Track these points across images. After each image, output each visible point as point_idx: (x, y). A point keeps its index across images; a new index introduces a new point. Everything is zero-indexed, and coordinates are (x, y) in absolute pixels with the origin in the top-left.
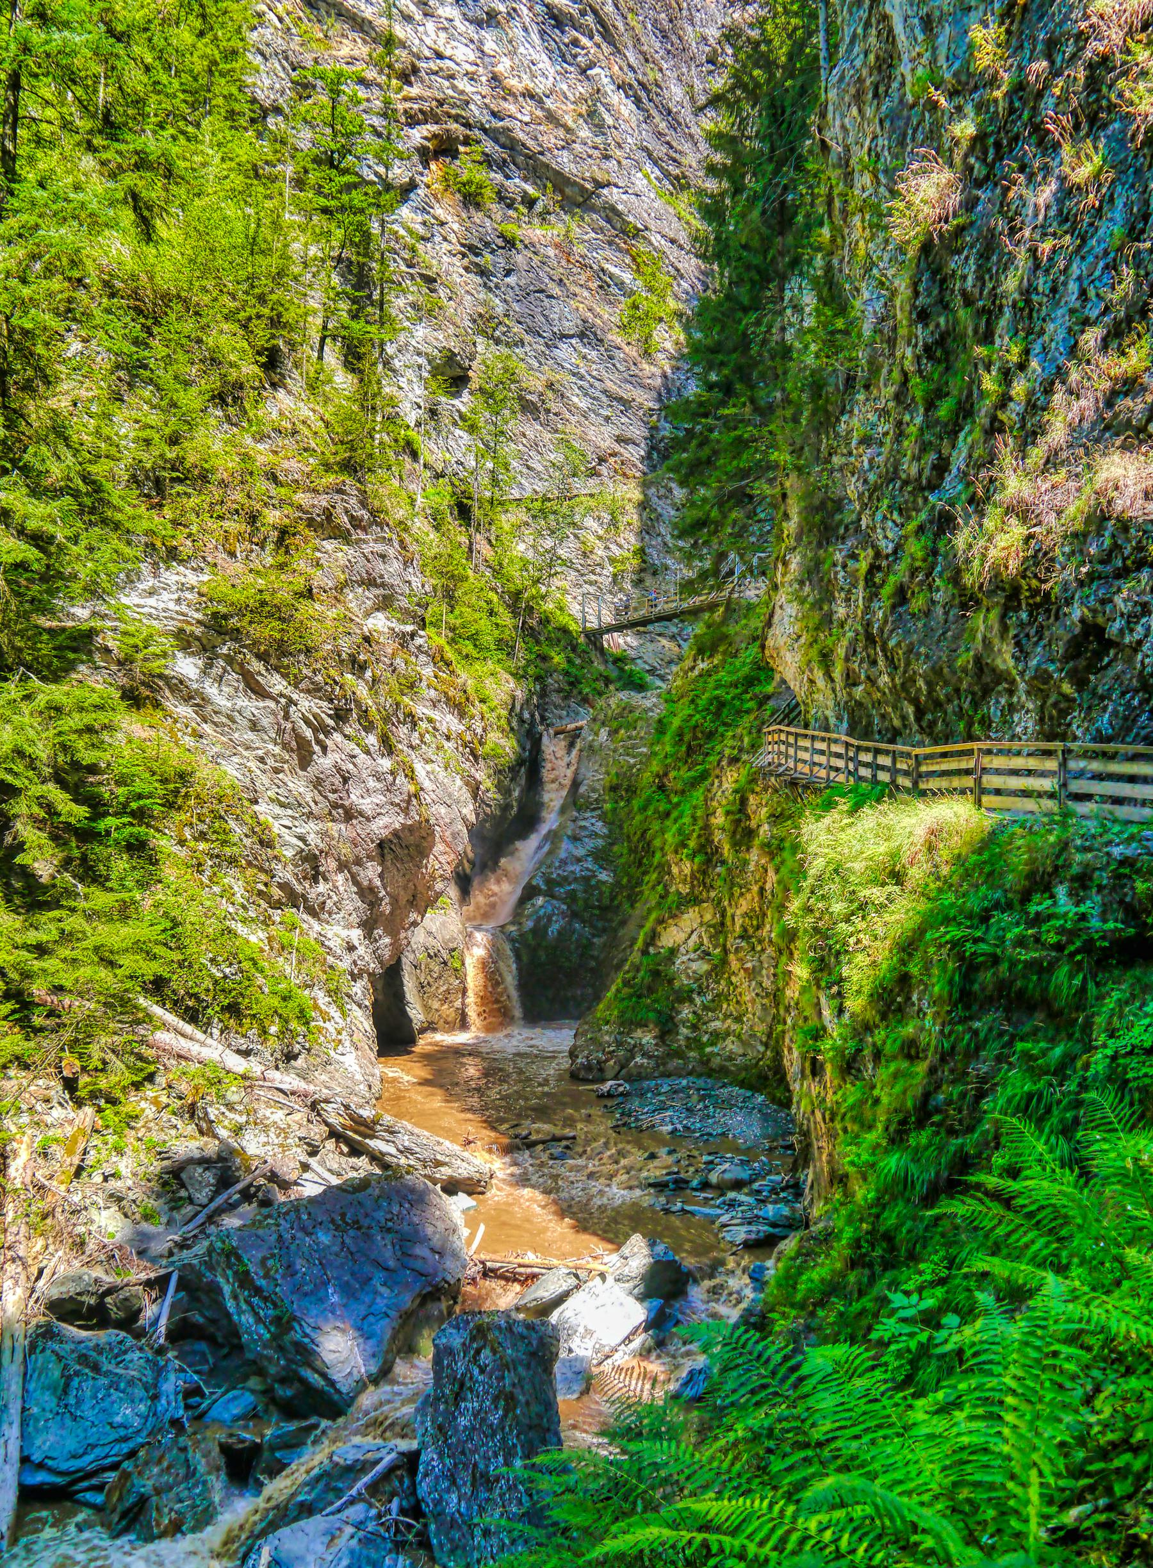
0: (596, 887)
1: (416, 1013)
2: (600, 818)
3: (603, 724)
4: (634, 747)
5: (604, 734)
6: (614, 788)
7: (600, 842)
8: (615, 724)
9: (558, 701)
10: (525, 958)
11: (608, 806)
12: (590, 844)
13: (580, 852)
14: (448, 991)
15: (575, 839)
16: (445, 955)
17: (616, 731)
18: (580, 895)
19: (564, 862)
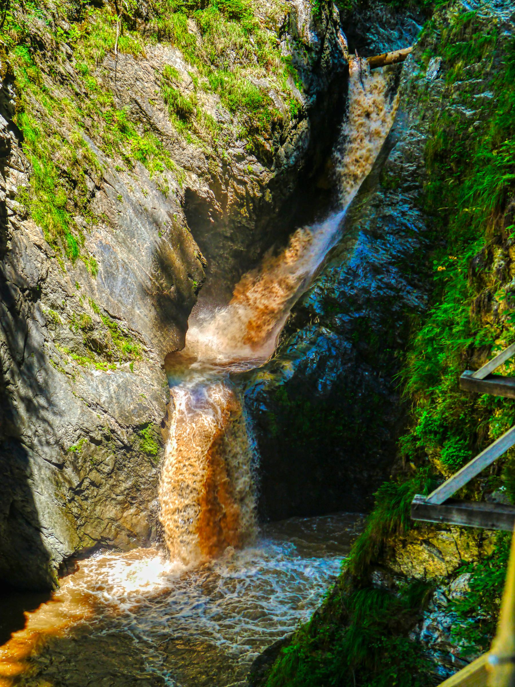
0: (400, 316)
1: (56, 541)
2: (415, 204)
3: (435, 51)
4: (474, 89)
5: (434, 66)
6: (440, 157)
7: (411, 244)
8: (449, 52)
9: (386, 16)
10: (274, 428)
11: (429, 185)
12: (396, 244)
13: (381, 257)
14: (136, 487)
15: (374, 235)
16: (124, 436)
17: (452, 62)
18: (374, 326)
19: (353, 273)
